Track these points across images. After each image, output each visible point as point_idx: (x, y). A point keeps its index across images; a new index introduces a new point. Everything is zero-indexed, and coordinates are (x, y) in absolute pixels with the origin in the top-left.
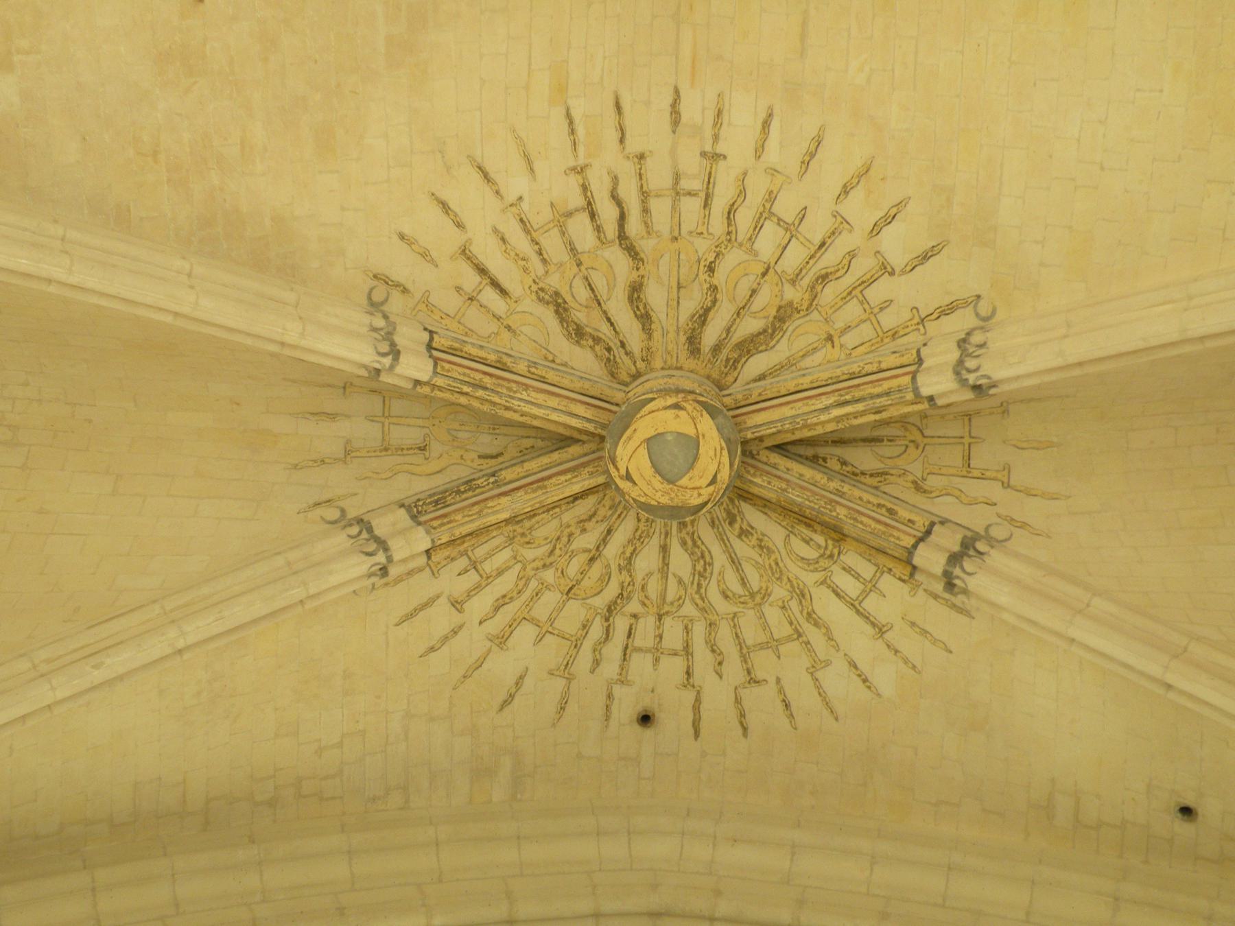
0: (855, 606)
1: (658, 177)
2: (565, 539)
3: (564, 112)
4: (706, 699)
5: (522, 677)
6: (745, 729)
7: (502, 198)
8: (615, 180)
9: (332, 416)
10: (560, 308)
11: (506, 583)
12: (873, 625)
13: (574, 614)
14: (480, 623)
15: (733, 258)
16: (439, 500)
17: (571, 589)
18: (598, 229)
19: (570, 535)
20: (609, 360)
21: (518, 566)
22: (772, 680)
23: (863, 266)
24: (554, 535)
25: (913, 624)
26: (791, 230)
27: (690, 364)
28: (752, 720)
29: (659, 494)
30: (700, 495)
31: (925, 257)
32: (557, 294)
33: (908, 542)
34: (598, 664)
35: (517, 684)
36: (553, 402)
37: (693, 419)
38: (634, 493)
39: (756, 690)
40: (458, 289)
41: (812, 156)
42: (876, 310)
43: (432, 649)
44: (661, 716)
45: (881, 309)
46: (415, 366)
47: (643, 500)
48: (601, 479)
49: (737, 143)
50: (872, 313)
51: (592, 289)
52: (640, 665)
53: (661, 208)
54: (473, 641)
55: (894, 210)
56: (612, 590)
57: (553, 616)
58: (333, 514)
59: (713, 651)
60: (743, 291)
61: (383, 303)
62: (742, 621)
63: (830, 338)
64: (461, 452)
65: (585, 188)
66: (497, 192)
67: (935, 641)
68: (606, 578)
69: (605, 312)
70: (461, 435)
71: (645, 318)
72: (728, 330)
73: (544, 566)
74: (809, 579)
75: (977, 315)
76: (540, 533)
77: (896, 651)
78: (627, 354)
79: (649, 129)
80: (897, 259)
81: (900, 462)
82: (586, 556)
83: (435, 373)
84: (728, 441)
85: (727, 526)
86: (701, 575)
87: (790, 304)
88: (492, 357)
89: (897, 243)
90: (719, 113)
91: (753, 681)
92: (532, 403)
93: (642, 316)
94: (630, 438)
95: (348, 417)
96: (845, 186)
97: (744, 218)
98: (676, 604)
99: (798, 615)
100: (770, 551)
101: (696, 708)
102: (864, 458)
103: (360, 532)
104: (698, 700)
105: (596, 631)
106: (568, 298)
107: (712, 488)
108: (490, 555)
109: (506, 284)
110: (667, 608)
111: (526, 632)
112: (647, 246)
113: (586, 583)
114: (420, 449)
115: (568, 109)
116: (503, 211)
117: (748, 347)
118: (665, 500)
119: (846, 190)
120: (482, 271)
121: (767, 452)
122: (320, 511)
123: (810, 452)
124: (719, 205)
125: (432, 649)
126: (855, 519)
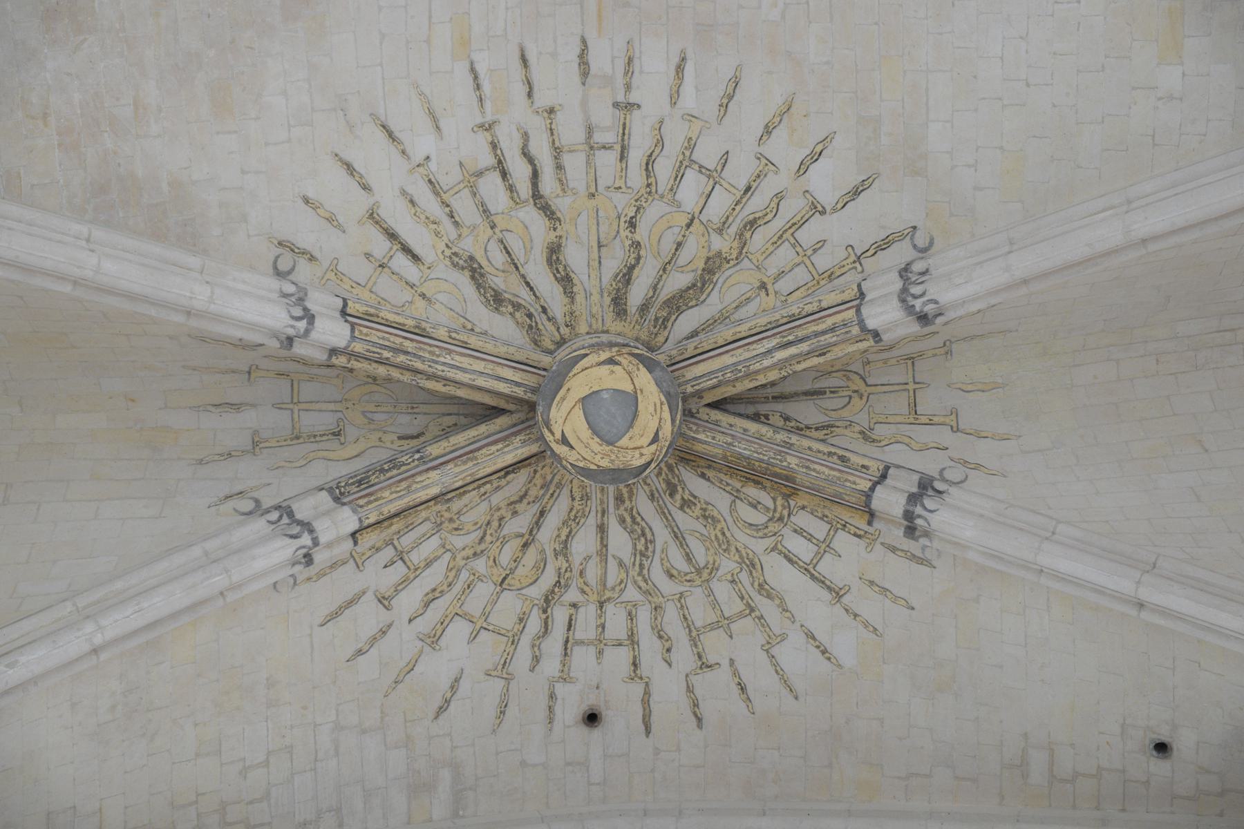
1: (571, 131)
2: (495, 524)
3: (468, 66)
4: (654, 690)
5: (457, 680)
6: (699, 720)
7: (409, 158)
8: (526, 137)
9: (236, 407)
10: (476, 273)
12: (829, 588)
13: (507, 609)
14: (410, 621)
15: (654, 210)
16: (362, 481)
17: (505, 579)
18: (511, 189)
19: (501, 519)
20: (530, 327)
21: (448, 556)
23: (792, 207)
24: (483, 519)
25: (872, 583)
26: (713, 176)
27: (617, 326)
28: (706, 709)
29: (598, 457)
30: (642, 455)
31: (856, 192)
32: (472, 258)
33: (865, 485)
34: (538, 661)
35: (452, 687)
36: (479, 366)
37: (629, 373)
38: (572, 457)
39: (709, 675)
40: (368, 256)
41: (731, 98)
42: (809, 252)
43: (360, 652)
44: (607, 715)
45: (815, 251)
47: (581, 464)
48: (534, 448)
50: (806, 255)
51: (508, 252)
52: (583, 658)
53: (575, 164)
54: (403, 641)
55: (818, 149)
56: (548, 579)
57: (488, 609)
58: (248, 505)
59: (660, 637)
60: (668, 245)
61: (289, 273)
62: (690, 601)
63: (763, 286)
64: (380, 434)
65: (494, 146)
66: (403, 152)
67: (895, 599)
68: (541, 566)
69: (523, 277)
70: (377, 417)
71: (566, 281)
72: (655, 288)
73: (475, 554)
74: (760, 546)
75: (915, 246)
76: (468, 518)
77: (856, 615)
78: (549, 319)
79: (555, 80)
80: (827, 197)
81: (845, 413)
82: (519, 542)
83: (353, 337)
84: (668, 395)
85: (667, 498)
86: (642, 554)
87: (719, 254)
89: (825, 181)
90: (630, 61)
91: (706, 666)
92: (458, 368)
93: (562, 279)
94: (563, 399)
95: (253, 406)
96: (767, 126)
97: (664, 170)
98: (618, 589)
99: (749, 588)
100: (715, 521)
102: (807, 412)
103: (281, 517)
104: (647, 693)
106: (484, 263)
107: (654, 447)
109: (418, 250)
110: (608, 594)
111: (460, 629)
112: (562, 205)
113: (520, 571)
114: (334, 434)
115: (472, 63)
116: (411, 171)
117: (677, 303)
118: (605, 463)
119: (768, 131)
120: (392, 236)
121: (707, 410)
122: (231, 504)
123: (751, 410)
124: (636, 156)
125: (360, 652)
126: (807, 467)
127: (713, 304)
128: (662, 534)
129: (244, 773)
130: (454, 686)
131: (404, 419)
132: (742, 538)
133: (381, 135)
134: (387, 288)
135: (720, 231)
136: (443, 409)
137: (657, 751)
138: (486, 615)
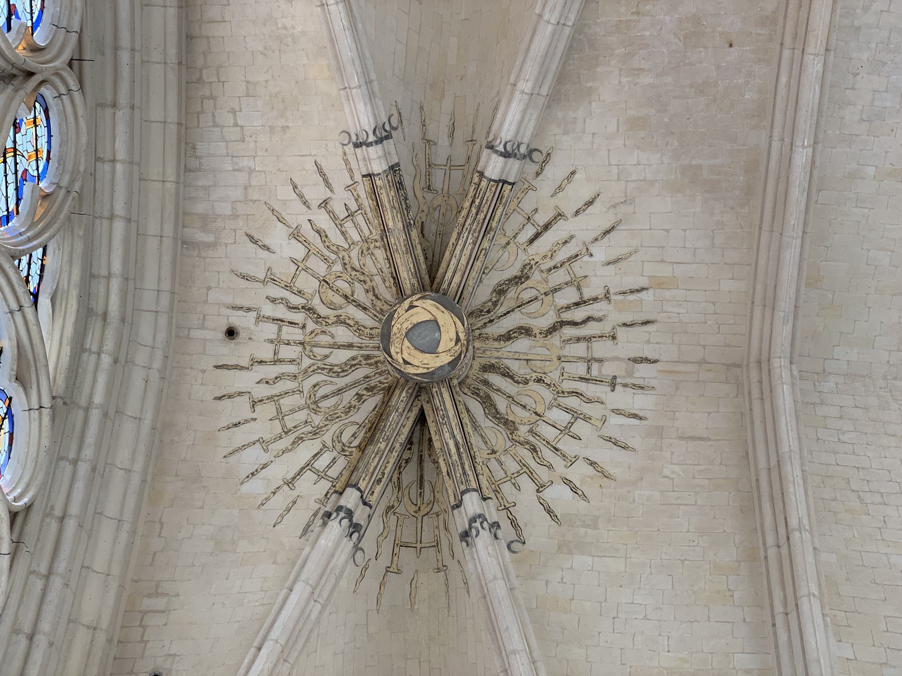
0: (308, 466)
1: (600, 349)
2: (362, 278)
3: (645, 286)
4: (244, 373)
5: (268, 249)
6: (220, 398)
7: (592, 243)
8: (599, 320)
9: (451, 135)
10: (519, 279)
11: (335, 237)
12: (294, 478)
14: (310, 220)
15: (547, 395)
16: (399, 186)
17: (327, 283)
18: (568, 308)
19: (365, 282)
20: (482, 311)
21: (346, 246)
22: (254, 416)
23: (543, 474)
24: (366, 270)
25: (295, 502)
26: (566, 430)
27: (476, 365)
28: (226, 402)
29: (399, 326)
30: (397, 353)
31: (549, 511)
32: (528, 278)
33: (362, 485)
34: (272, 302)
35: (264, 246)
36: (463, 261)
37: (449, 350)
38: (401, 311)
39: (248, 406)
40: (536, 210)
41: (615, 444)
42: (513, 481)
43: (295, 187)
44: (232, 344)
45: (514, 484)
46: (494, 166)
47: (396, 316)
48: (408, 292)
49: (622, 398)
51: (529, 302)
52: (270, 330)
53: (580, 349)
54: (298, 215)
55: (578, 492)
56: (323, 311)
57: (310, 271)
58: (395, 122)
59: (276, 378)
60: (524, 400)
61: (531, 159)
62: (297, 396)
63: (494, 452)
64: (426, 211)
65: (595, 299)
66: (596, 239)
67: (282, 516)
68: (332, 306)
69: (513, 310)
70: (437, 213)
71: (508, 337)
72: (498, 390)
73: (345, 264)
74: (327, 438)
75: (512, 542)
76: (368, 260)
77: (274, 493)
78: (485, 324)
79: (632, 342)
80: (547, 494)
81: (406, 499)
82: (349, 293)
83: (490, 180)
84: (433, 373)
85: (365, 386)
86: (330, 370)
87: (517, 429)
88: (494, 224)
89: (558, 494)
90: (642, 388)
91: (254, 404)
92: (464, 246)
93: (509, 335)
94: (438, 308)
95: (451, 145)
96: (595, 463)
97: (572, 402)
98: (311, 354)
99: (300, 432)
100: (346, 413)
101: (237, 367)
102: (409, 475)
103: (386, 131)
105: (296, 300)
106: (524, 286)
107: (401, 361)
108: (356, 226)
109: (536, 243)
110: (308, 348)
111: (299, 251)
113: (330, 293)
114: (429, 186)
115: (647, 289)
116: (584, 243)
117: (488, 403)
118: (395, 330)
119: (592, 464)
120: (547, 227)
121: (419, 406)
122: (396, 115)
123: (415, 440)
124: (581, 387)
125: (295, 187)
126: (377, 453)
127: (486, 423)
128: (341, 382)
129: (233, 112)
130: (266, 248)
131: (434, 228)
132: (334, 428)
133: (607, 226)
134: (516, 220)
135: (531, 431)
136: (437, 251)
137: (203, 371)
138: (306, 269)
